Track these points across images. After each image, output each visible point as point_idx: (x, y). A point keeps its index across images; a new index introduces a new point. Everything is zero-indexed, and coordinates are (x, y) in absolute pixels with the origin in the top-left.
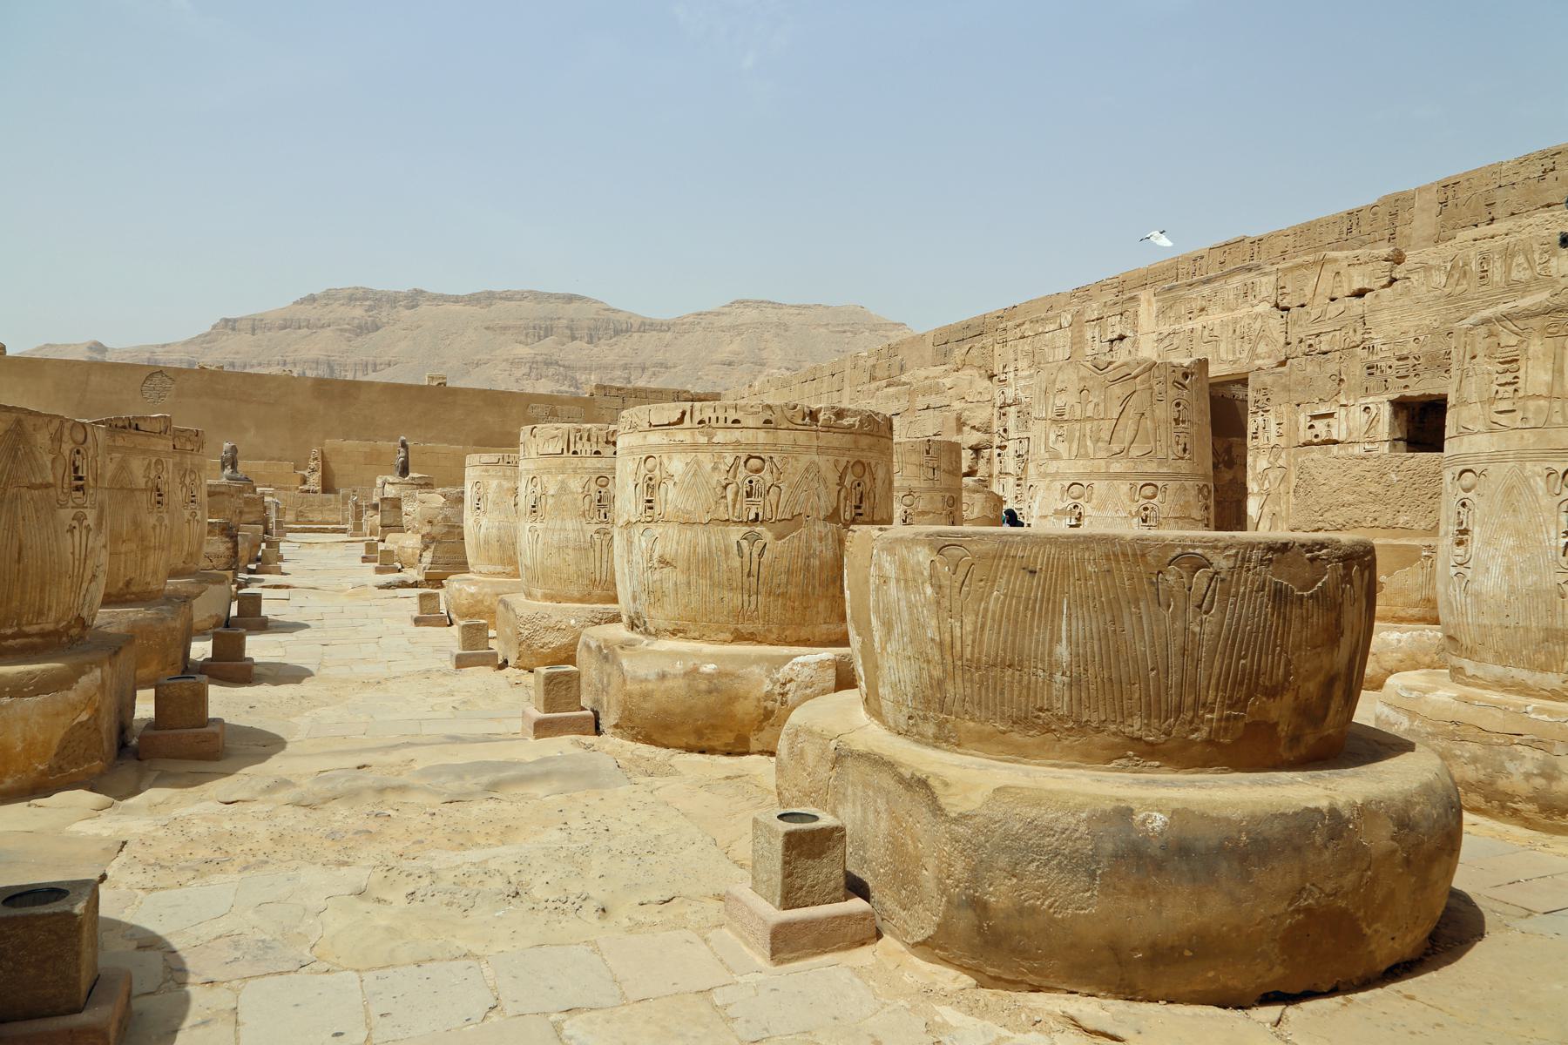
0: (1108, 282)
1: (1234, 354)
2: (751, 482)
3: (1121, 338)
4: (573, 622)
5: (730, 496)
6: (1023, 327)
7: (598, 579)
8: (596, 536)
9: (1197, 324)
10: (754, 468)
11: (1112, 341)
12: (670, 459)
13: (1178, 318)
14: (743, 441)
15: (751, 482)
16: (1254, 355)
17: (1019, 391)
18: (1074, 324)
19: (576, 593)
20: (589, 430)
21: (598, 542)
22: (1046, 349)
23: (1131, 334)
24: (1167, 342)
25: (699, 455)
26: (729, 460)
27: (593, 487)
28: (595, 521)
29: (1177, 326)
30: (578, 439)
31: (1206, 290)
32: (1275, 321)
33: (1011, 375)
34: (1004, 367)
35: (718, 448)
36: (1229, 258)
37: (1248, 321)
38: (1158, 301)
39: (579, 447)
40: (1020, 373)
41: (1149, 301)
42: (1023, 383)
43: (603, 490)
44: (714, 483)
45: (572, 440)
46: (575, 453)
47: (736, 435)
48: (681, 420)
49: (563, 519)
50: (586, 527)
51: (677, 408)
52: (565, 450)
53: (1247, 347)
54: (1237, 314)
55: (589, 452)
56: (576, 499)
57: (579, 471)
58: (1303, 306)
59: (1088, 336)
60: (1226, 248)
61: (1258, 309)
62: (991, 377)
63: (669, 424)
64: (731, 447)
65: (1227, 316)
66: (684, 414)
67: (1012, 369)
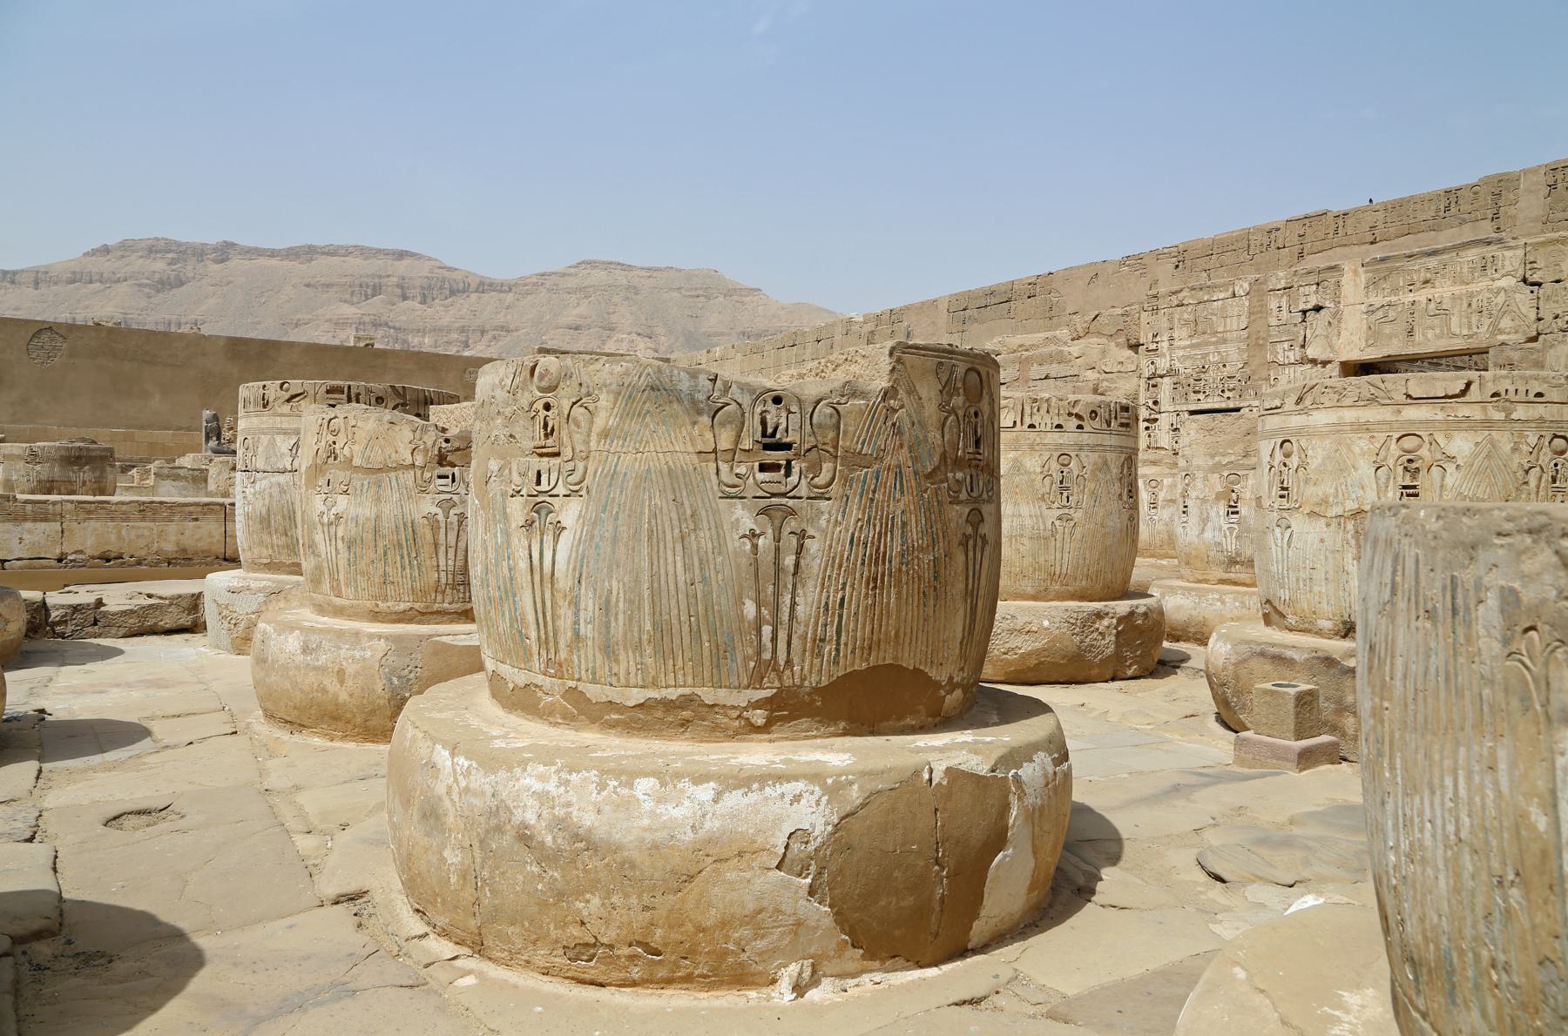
0: (1165, 251)
1: (1470, 328)
2: (1556, 465)
3: (1318, 309)
4: (1046, 623)
5: (1533, 483)
6: (1181, 295)
7: (1058, 573)
8: (1057, 523)
9: (1421, 296)
10: (1559, 449)
11: (1304, 312)
12: (1448, 437)
13: (1395, 291)
14: (1548, 417)
15: (1556, 465)
16: (1496, 329)
17: (1176, 362)
18: (1252, 293)
19: (1029, 589)
20: (1047, 400)
21: (1060, 530)
22: (1214, 318)
23: (1332, 305)
24: (1380, 314)
25: (1494, 433)
26: (1533, 440)
27: (1054, 466)
28: (1056, 505)
29: (1393, 298)
30: (1035, 410)
31: (1432, 262)
32: (1524, 297)
33: (1165, 345)
34: (1155, 336)
35: (1518, 426)
36: (1309, 231)
37: (1488, 295)
38: (1367, 272)
39: (1036, 420)
40: (1176, 343)
41: (1355, 272)
42: (1181, 353)
43: (1066, 470)
44: (1515, 466)
45: (1027, 410)
46: (1032, 426)
47: (1540, 411)
48: (1463, 393)
49: (1015, 504)
50: (1046, 512)
51: (1457, 378)
52: (1019, 423)
53: (1487, 322)
54: (1473, 288)
55: (1049, 425)
56: (1033, 480)
57: (1037, 448)
58: (1558, 281)
59: (1273, 305)
60: (1306, 221)
61: (1504, 283)
62: (1135, 347)
63: (1446, 397)
64: (1534, 425)
65: (1459, 289)
66: (1468, 385)
67: (1165, 338)
